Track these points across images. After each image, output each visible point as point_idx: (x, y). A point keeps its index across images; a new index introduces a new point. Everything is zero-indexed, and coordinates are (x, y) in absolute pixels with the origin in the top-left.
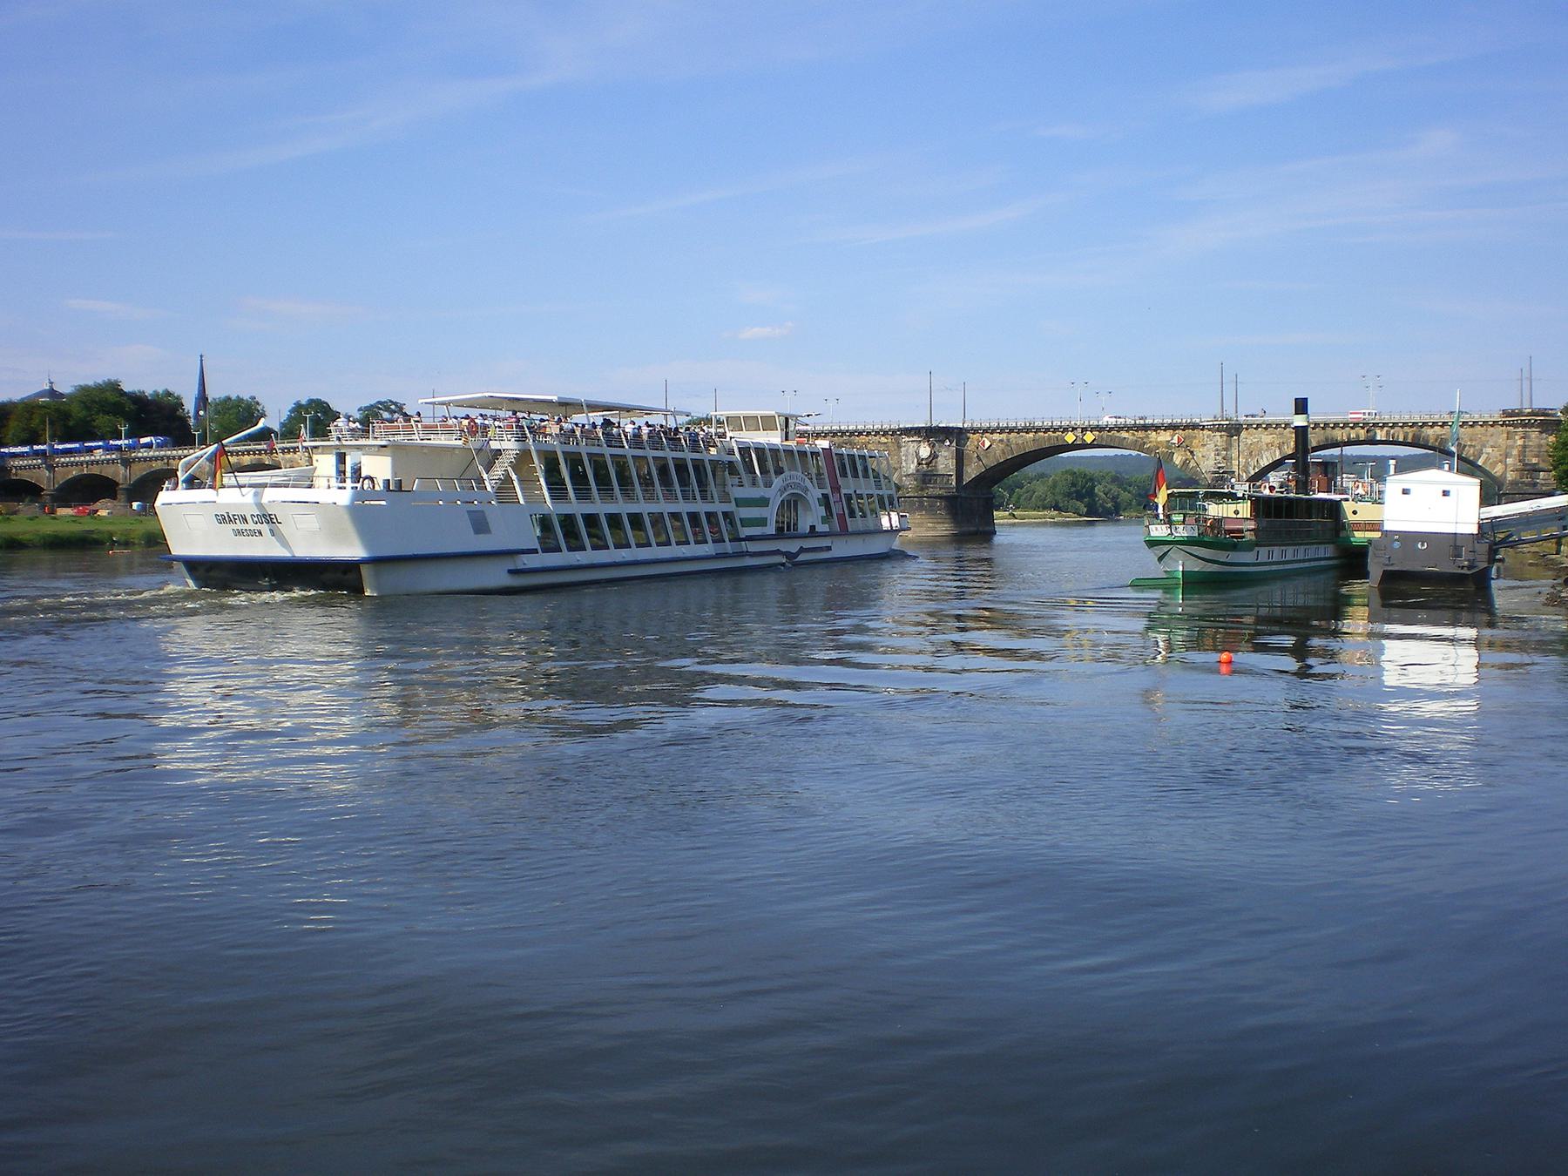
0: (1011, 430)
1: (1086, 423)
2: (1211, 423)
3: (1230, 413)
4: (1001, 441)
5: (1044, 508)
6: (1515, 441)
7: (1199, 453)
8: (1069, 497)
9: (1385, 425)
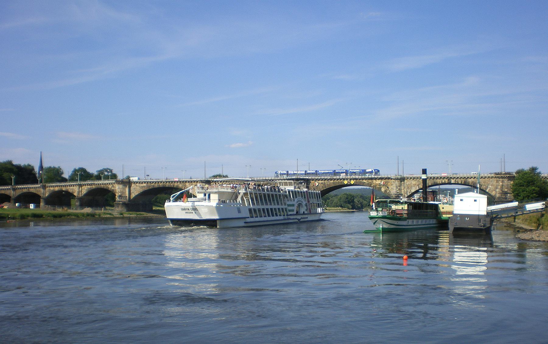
2: (395, 177)
3: (401, 173)
4: (322, 183)
5: (337, 206)
6: (499, 183)
7: (390, 187)
9: (454, 178)
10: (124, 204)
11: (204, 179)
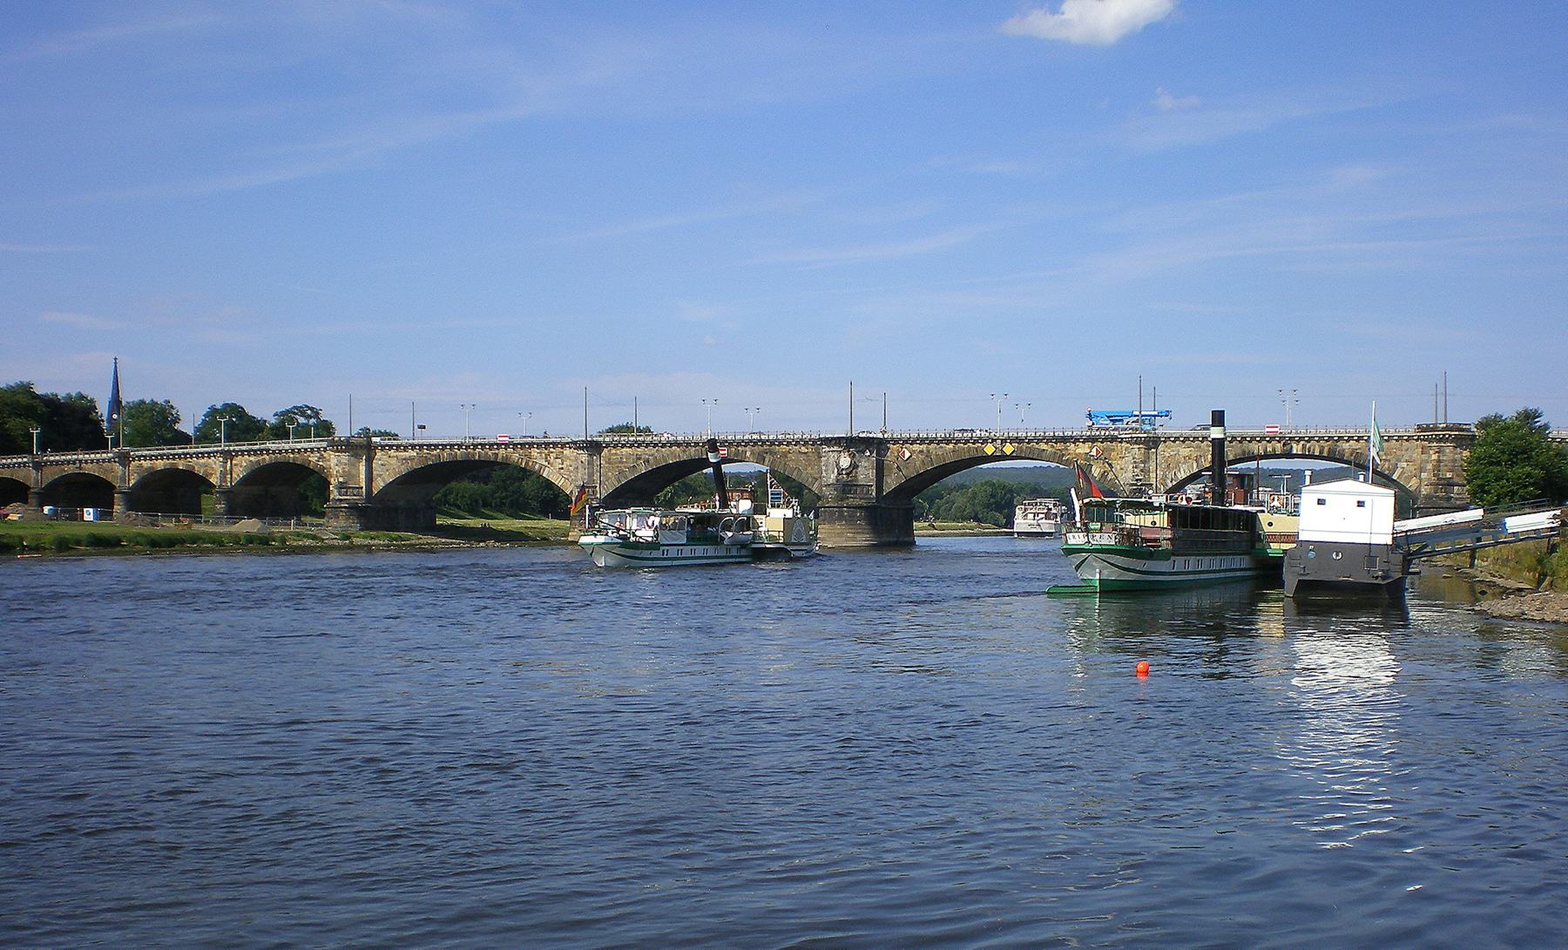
0: (932, 442)
1: (1006, 435)
2: (1130, 436)
4: (921, 452)
5: (964, 519)
6: (1430, 456)
7: (1117, 465)
8: (988, 508)
9: (1301, 439)
10: (354, 509)
11: (584, 439)
